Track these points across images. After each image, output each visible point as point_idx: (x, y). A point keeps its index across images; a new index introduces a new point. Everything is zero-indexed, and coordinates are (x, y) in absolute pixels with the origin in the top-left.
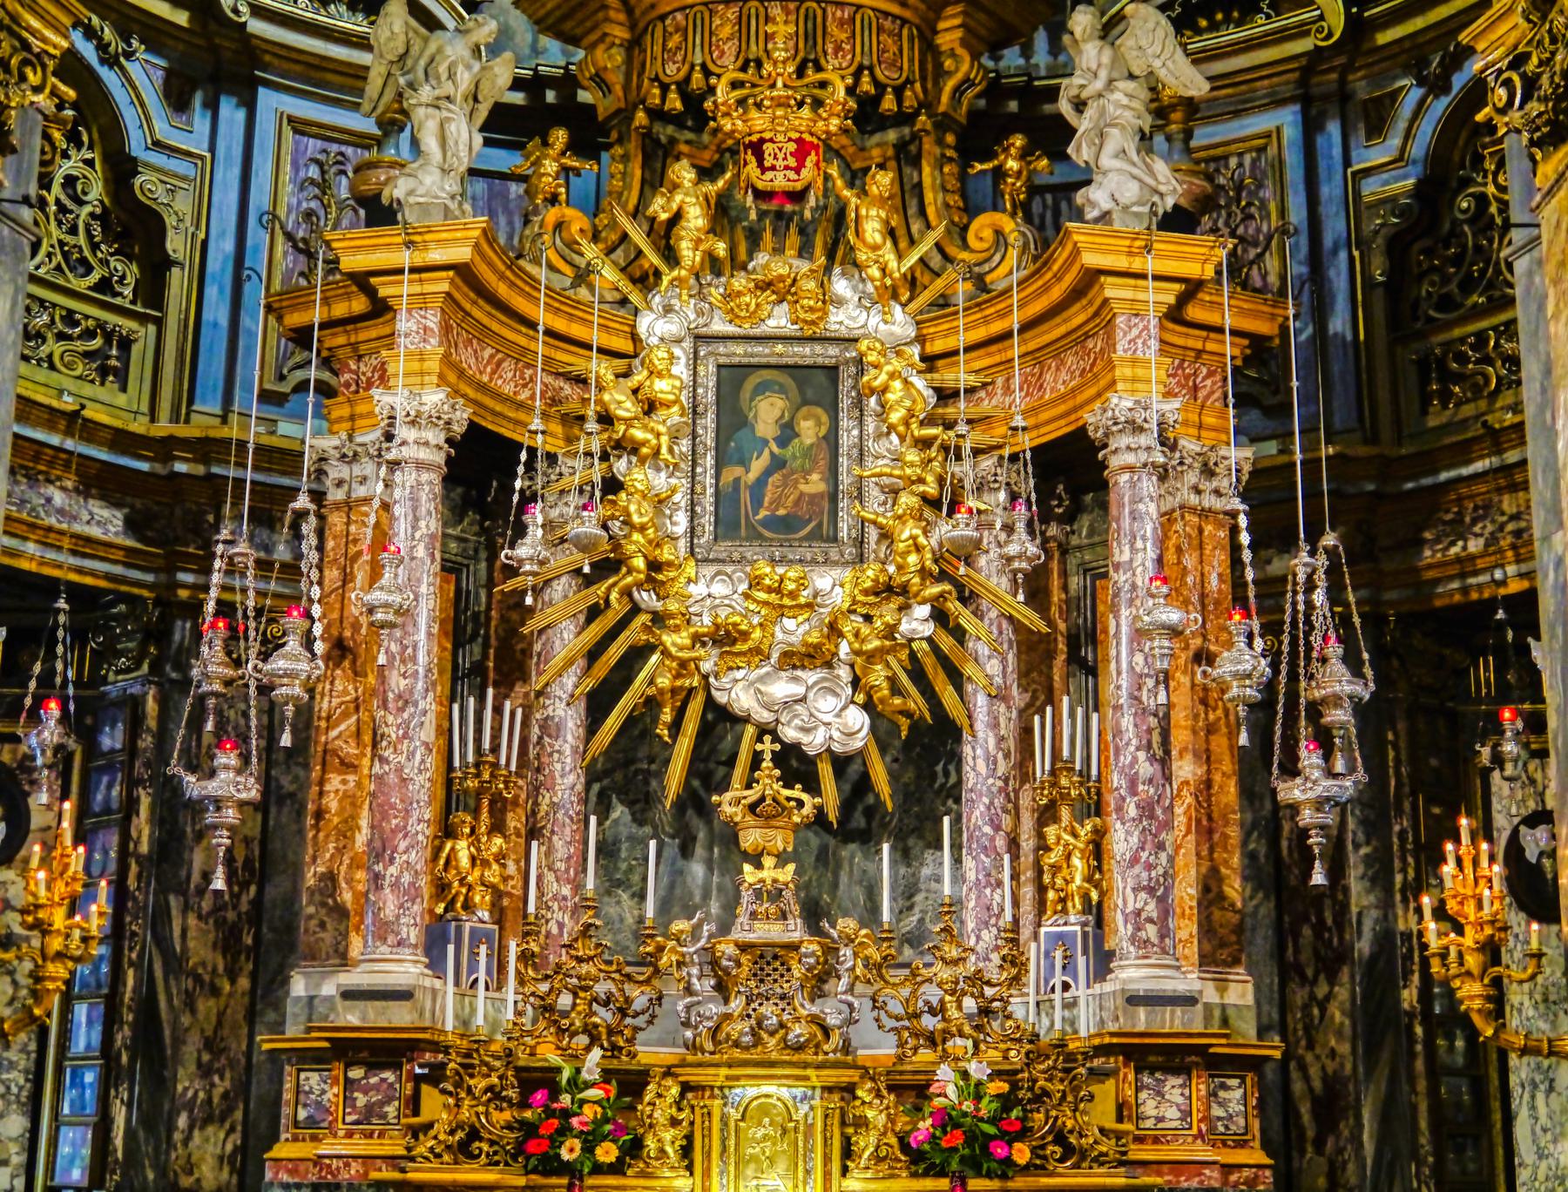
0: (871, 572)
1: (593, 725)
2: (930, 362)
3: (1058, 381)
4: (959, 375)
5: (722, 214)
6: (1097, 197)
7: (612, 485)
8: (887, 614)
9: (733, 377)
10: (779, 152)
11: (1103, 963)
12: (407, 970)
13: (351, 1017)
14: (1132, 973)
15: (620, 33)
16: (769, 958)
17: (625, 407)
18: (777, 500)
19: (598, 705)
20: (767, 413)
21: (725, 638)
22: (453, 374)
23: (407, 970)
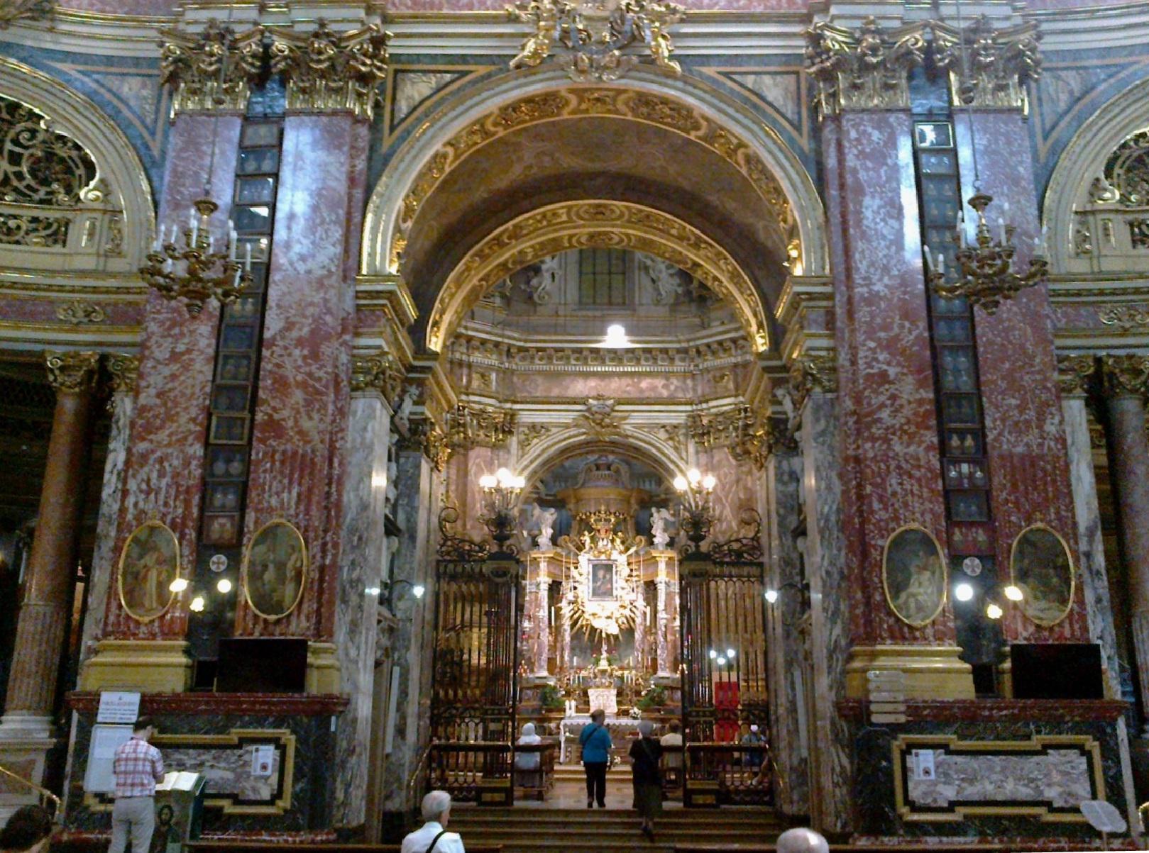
0: (619, 603)
1: (572, 628)
2: (629, 564)
3: (651, 570)
4: (634, 567)
5: (592, 538)
6: (656, 540)
7: (575, 588)
8: (622, 610)
9: (594, 566)
10: (603, 532)
11: (655, 671)
12: (544, 673)
13: (537, 681)
14: (661, 674)
15: (573, 501)
16: (604, 672)
17: (578, 578)
18: (603, 589)
19: (573, 626)
20: (601, 573)
21: (594, 615)
22: (550, 574)
23: (544, 673)
